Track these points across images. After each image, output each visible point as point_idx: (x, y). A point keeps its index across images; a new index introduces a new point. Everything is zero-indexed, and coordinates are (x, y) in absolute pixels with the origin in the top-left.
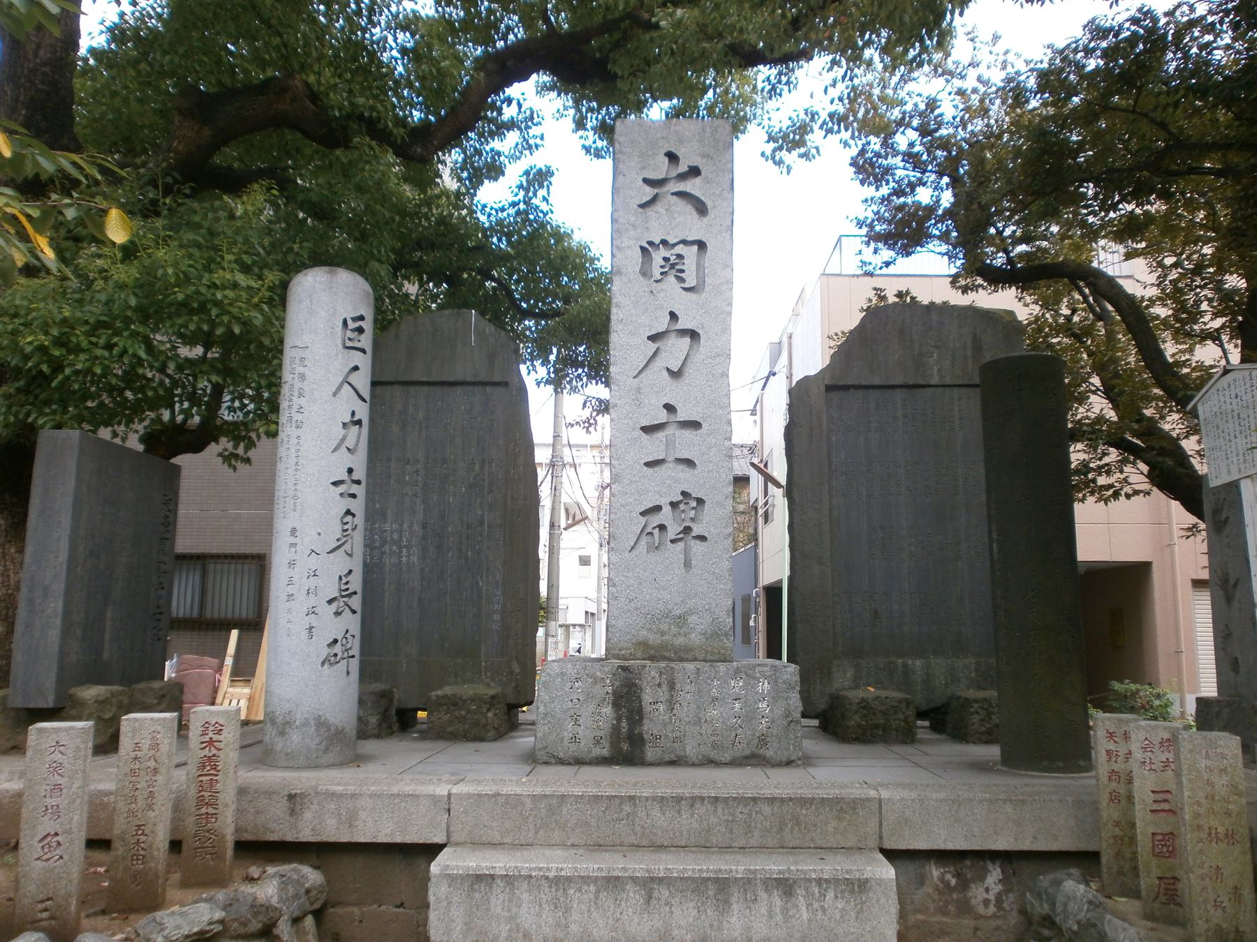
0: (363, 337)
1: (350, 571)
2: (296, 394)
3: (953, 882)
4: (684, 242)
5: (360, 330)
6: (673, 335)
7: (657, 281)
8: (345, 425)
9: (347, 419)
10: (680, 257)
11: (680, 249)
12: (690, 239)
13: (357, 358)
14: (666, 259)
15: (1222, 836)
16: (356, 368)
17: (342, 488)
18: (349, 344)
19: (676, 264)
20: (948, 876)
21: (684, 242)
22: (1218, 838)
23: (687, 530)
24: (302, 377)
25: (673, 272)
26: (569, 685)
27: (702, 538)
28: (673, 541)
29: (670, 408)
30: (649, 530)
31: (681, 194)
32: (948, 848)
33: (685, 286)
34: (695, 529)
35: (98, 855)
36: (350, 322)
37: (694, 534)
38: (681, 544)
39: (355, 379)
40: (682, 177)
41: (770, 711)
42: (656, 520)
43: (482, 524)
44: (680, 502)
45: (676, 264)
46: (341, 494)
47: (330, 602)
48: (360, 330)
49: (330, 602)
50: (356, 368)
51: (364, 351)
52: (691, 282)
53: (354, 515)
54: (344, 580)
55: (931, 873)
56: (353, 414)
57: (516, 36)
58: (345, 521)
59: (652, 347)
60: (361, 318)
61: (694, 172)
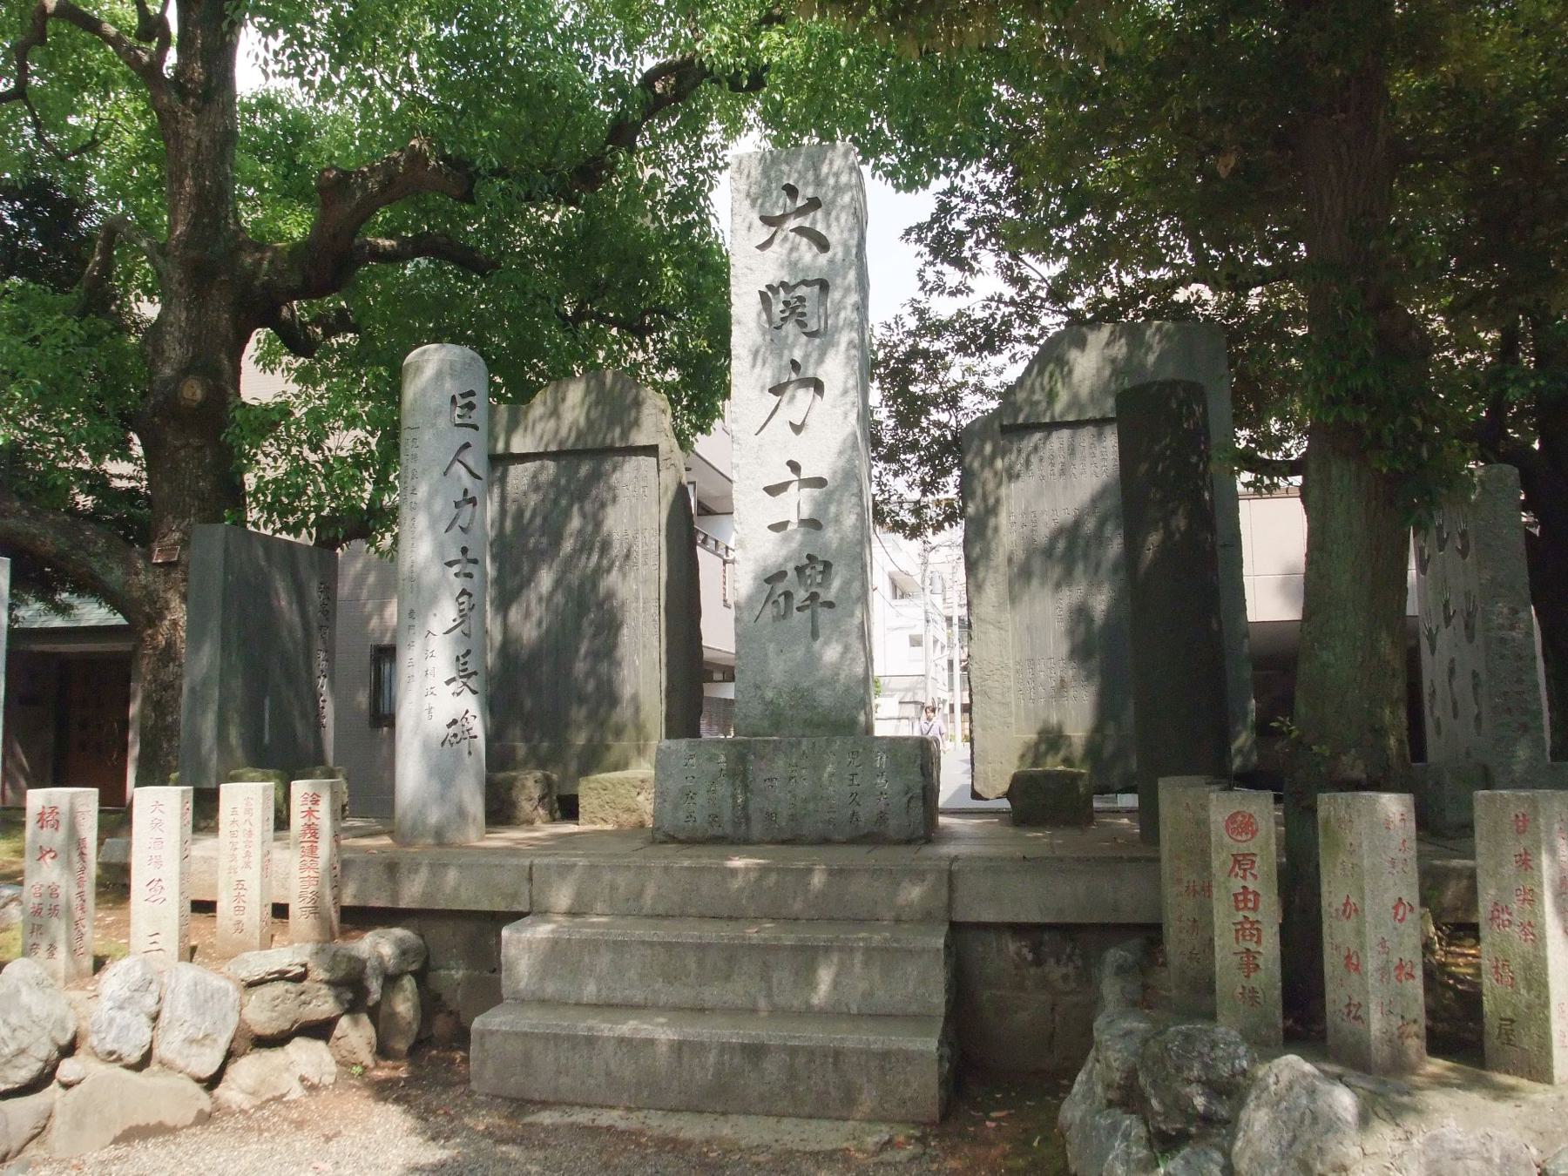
0: (474, 413)
1: (468, 652)
2: (410, 476)
3: (1030, 957)
4: (805, 283)
5: (470, 406)
6: (791, 387)
7: (777, 328)
8: (457, 505)
9: (460, 498)
10: (801, 299)
11: (802, 291)
12: (809, 278)
13: (467, 435)
14: (786, 303)
15: (1198, 888)
16: (467, 446)
17: (456, 569)
18: (458, 421)
19: (798, 307)
20: (1025, 951)
21: (805, 283)
22: (1195, 891)
23: (814, 597)
24: (415, 457)
25: (795, 317)
26: (683, 762)
27: (830, 605)
28: (799, 609)
29: (794, 467)
30: (775, 597)
31: (800, 231)
32: (1031, 920)
33: (807, 330)
34: (822, 595)
35: (201, 920)
36: (458, 398)
37: (820, 600)
38: (808, 612)
39: (469, 457)
40: (800, 212)
41: (889, 787)
42: (781, 588)
43: (637, 599)
44: (807, 566)
45: (798, 307)
46: (456, 575)
47: (448, 683)
48: (470, 406)
49: (448, 683)
50: (467, 446)
51: (476, 427)
52: (813, 325)
53: (470, 595)
54: (462, 661)
55: (1007, 946)
56: (466, 492)
57: (34, 73)
58: (461, 600)
59: (774, 399)
60: (471, 393)
61: (814, 204)
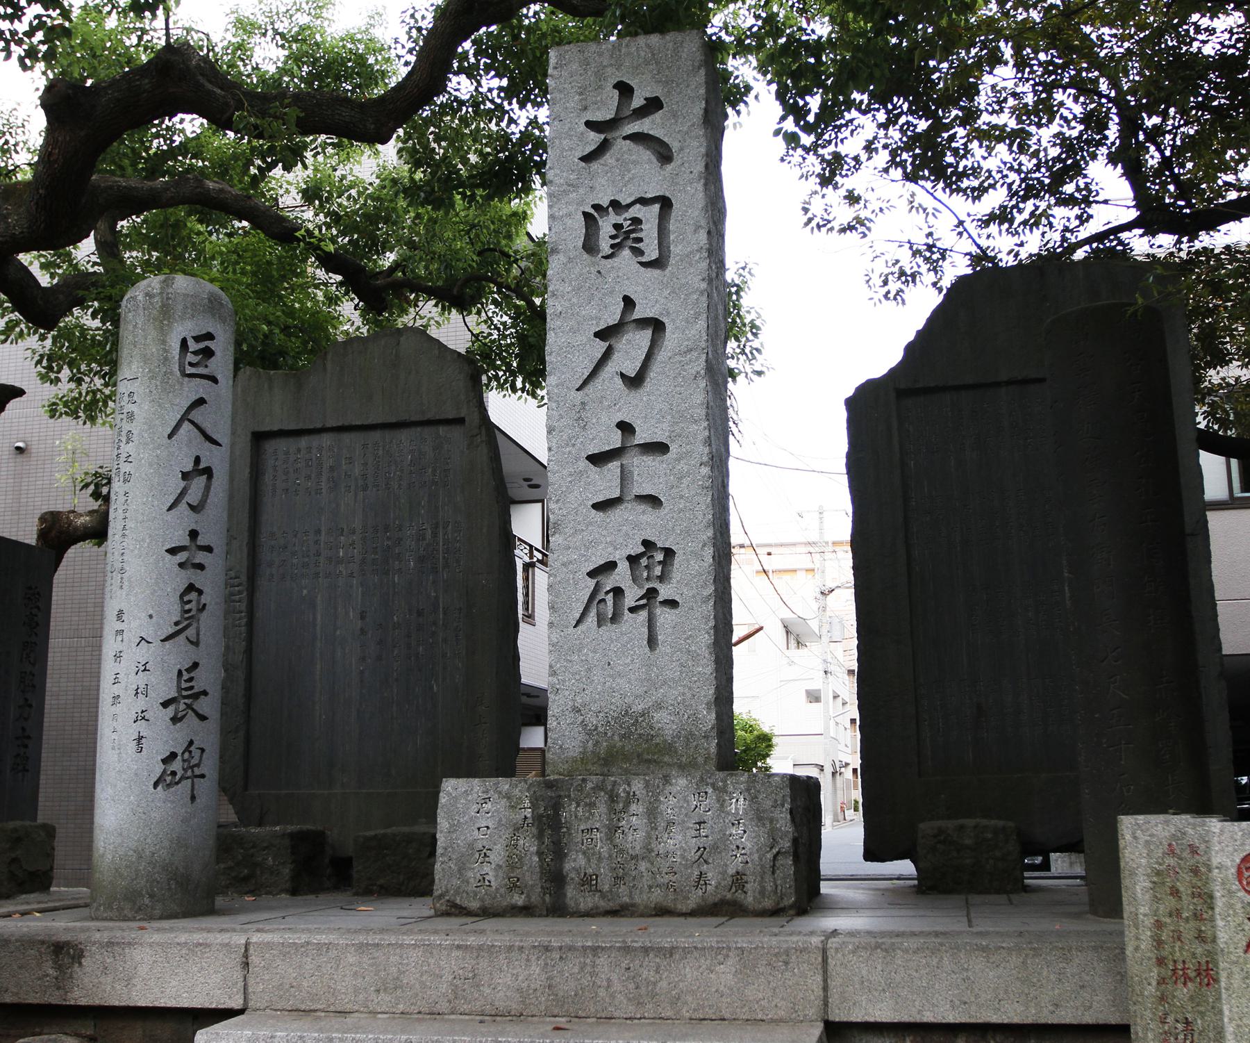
2: (124, 439)
4: (643, 201)
8: (185, 476)
9: (189, 467)
10: (636, 221)
11: (636, 211)
12: (649, 196)
14: (617, 227)
17: (182, 557)
18: (190, 370)
21: (643, 201)
23: (652, 593)
27: (672, 604)
28: (632, 610)
30: (601, 596)
31: (637, 138)
33: (644, 259)
34: (662, 591)
36: (191, 343)
37: (660, 598)
38: (643, 614)
40: (642, 112)
42: (609, 582)
46: (181, 565)
49: (165, 704)
50: (200, 402)
51: (214, 380)
53: (200, 592)
54: (186, 676)
58: (186, 599)
59: (601, 346)
60: (209, 336)
61: (653, 105)
